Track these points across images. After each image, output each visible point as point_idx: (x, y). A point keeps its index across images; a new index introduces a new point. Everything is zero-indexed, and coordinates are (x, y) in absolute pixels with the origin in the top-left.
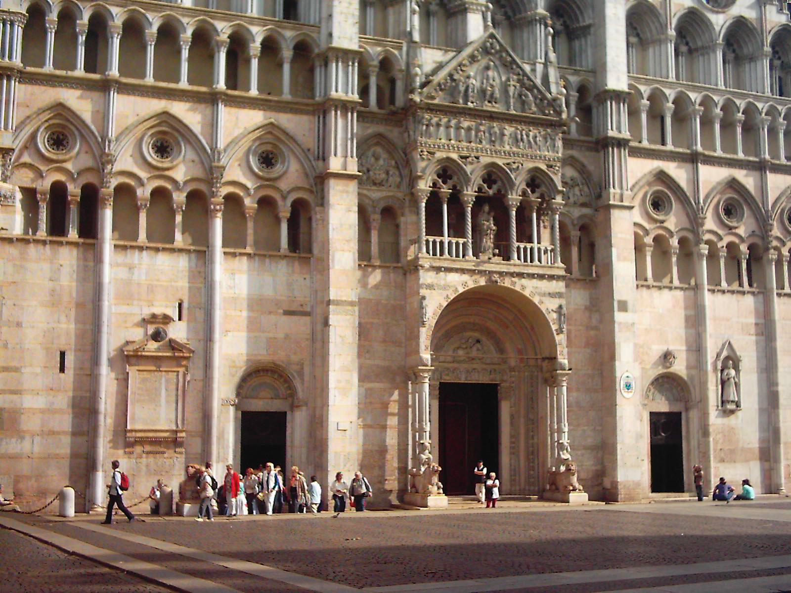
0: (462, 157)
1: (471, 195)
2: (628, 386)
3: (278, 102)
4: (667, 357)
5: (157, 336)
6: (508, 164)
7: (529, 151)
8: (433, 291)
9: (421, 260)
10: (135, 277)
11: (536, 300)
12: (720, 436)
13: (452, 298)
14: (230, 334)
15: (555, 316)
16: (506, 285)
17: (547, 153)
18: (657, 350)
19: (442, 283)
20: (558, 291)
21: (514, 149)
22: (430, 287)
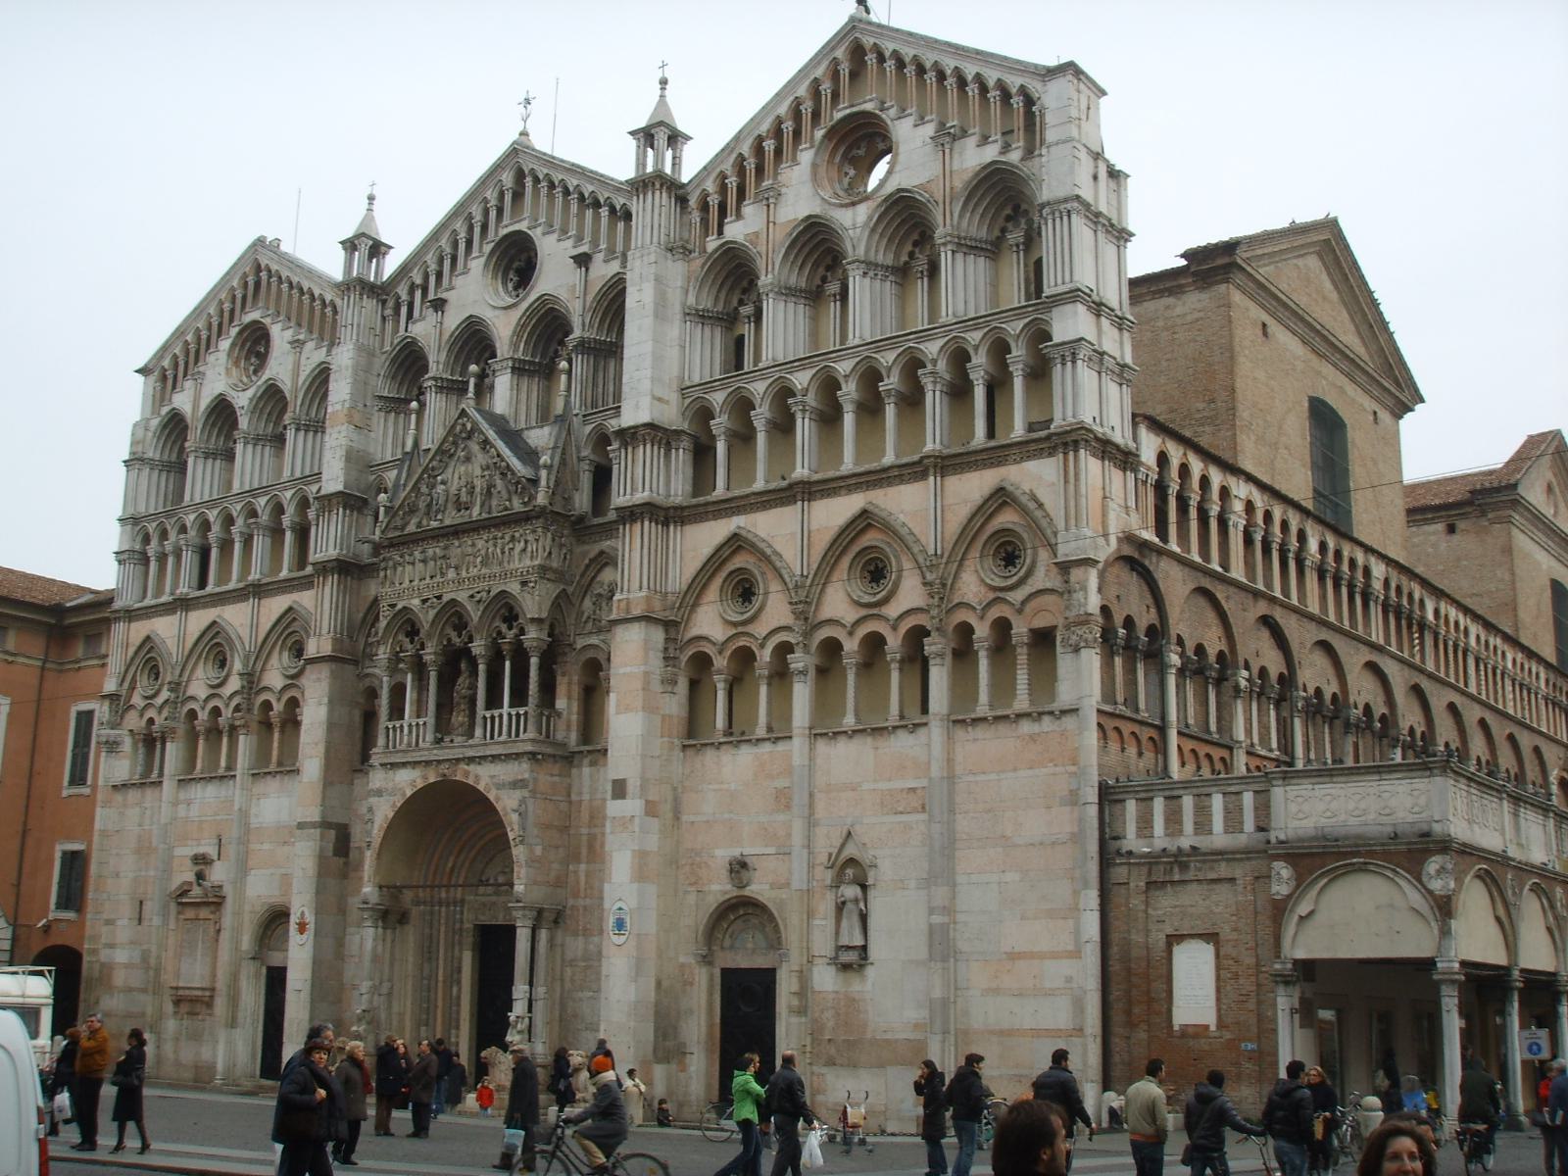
0: (424, 601)
1: (430, 654)
2: (620, 924)
3: (1048, 438)
4: (739, 867)
5: (200, 876)
6: (472, 596)
7: (496, 569)
8: (381, 799)
9: (374, 757)
10: (191, 814)
11: (491, 797)
12: (829, 1014)
13: (399, 805)
14: (253, 872)
15: (515, 817)
16: (459, 777)
17: (512, 566)
18: (724, 854)
19: (391, 784)
20: (520, 777)
21: (484, 571)
22: (379, 793)
